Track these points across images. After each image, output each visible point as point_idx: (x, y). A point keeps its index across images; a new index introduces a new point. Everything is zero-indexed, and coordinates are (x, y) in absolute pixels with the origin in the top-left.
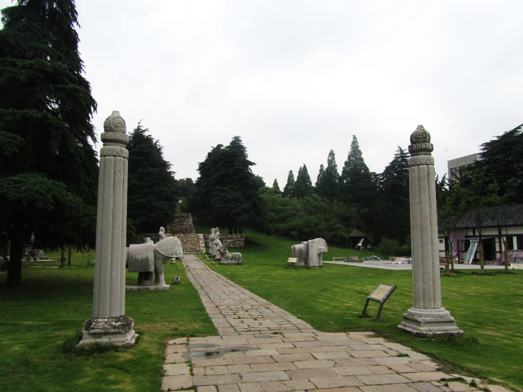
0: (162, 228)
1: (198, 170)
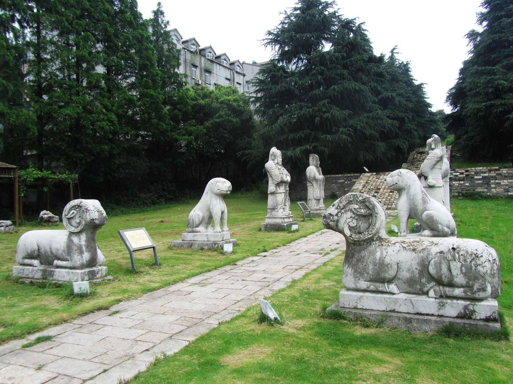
0: (274, 150)
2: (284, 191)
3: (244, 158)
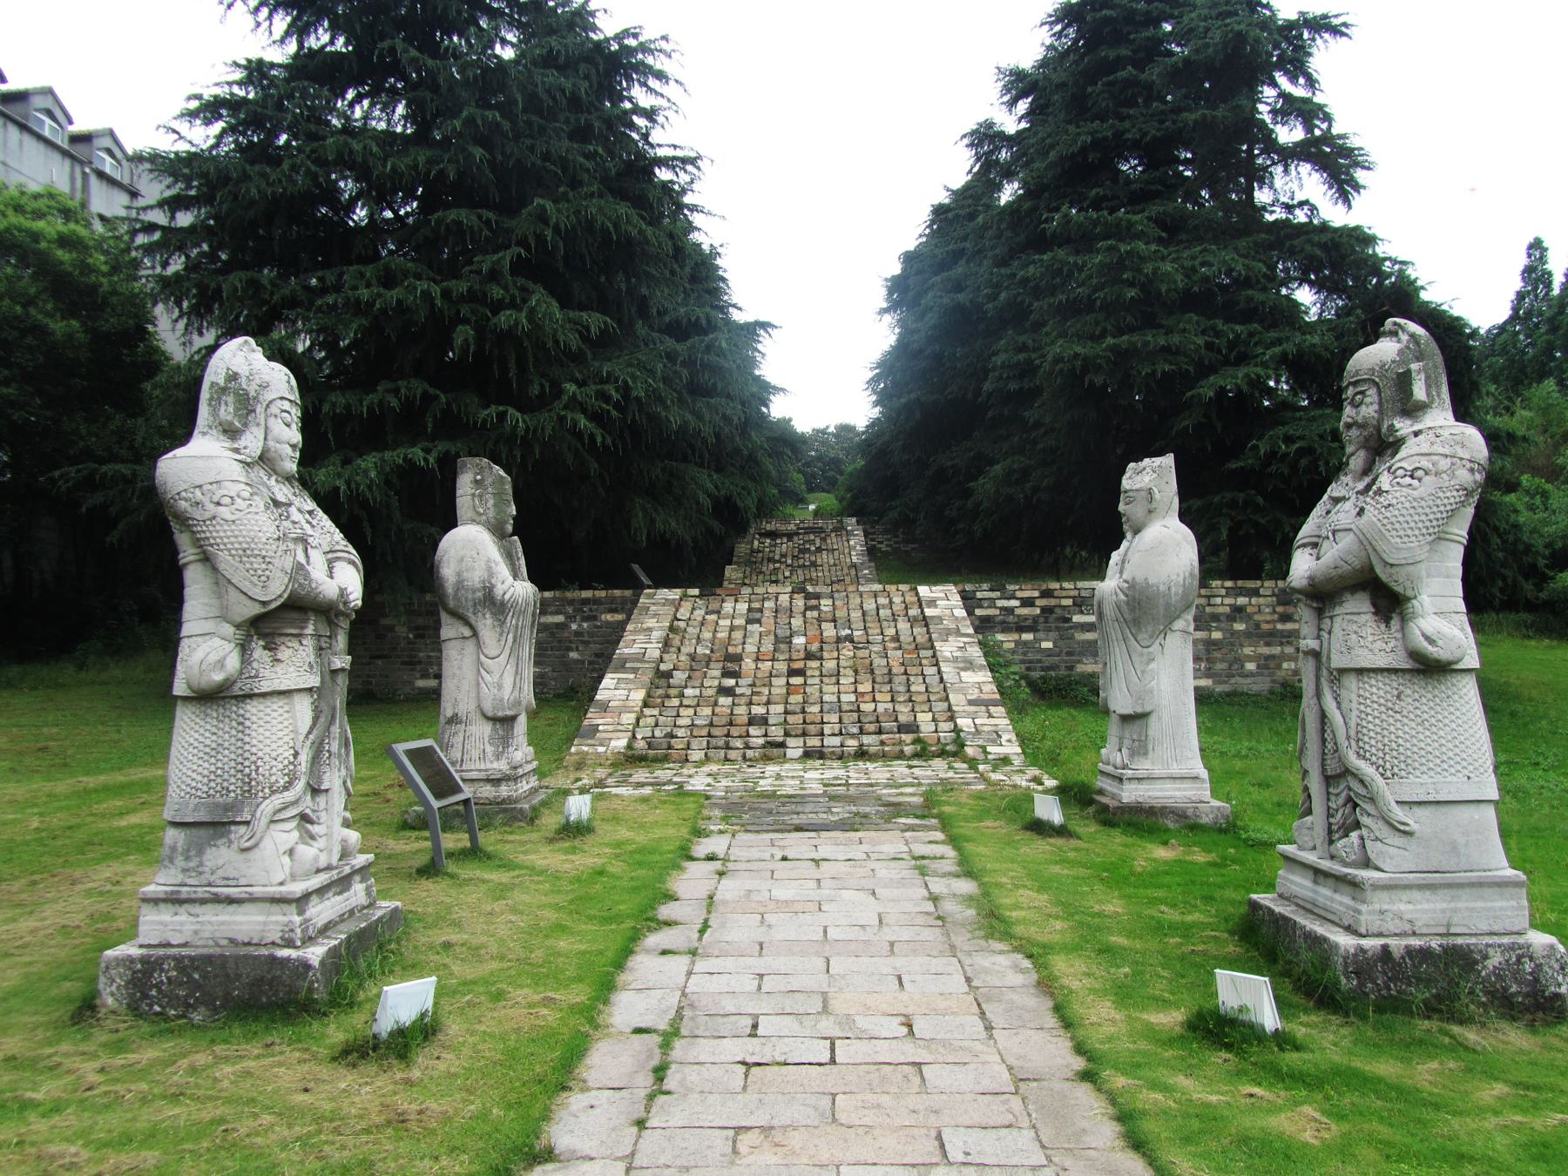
1: (883, 311)
2: (314, 681)
3: (97, 499)
